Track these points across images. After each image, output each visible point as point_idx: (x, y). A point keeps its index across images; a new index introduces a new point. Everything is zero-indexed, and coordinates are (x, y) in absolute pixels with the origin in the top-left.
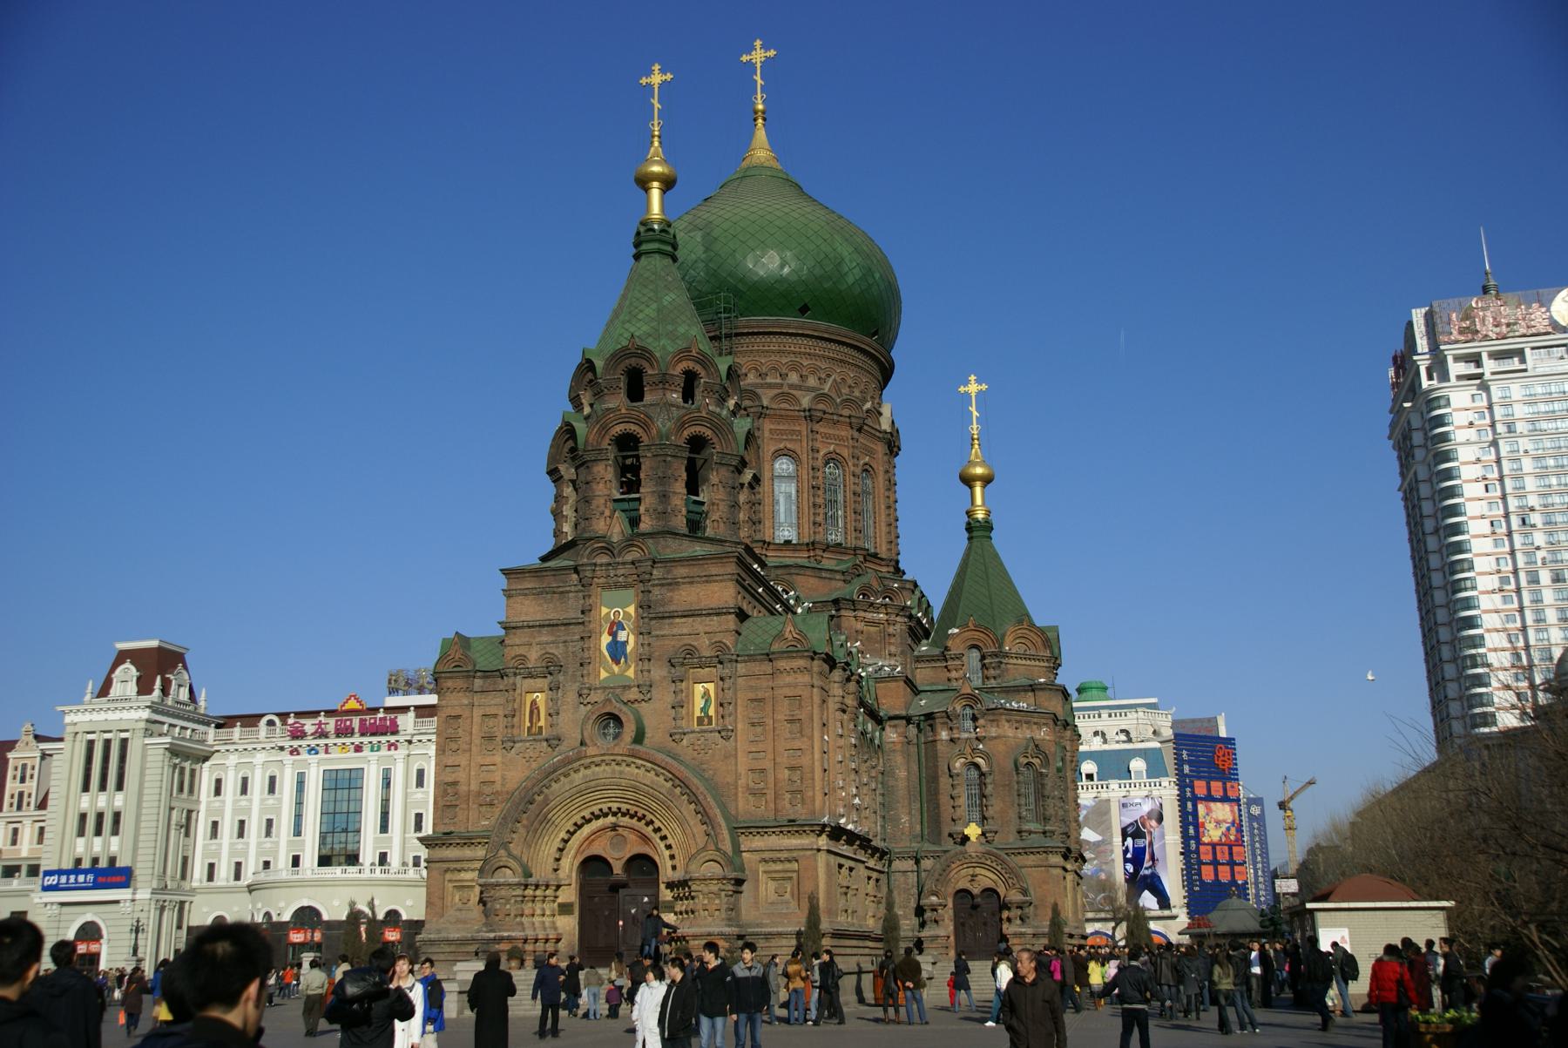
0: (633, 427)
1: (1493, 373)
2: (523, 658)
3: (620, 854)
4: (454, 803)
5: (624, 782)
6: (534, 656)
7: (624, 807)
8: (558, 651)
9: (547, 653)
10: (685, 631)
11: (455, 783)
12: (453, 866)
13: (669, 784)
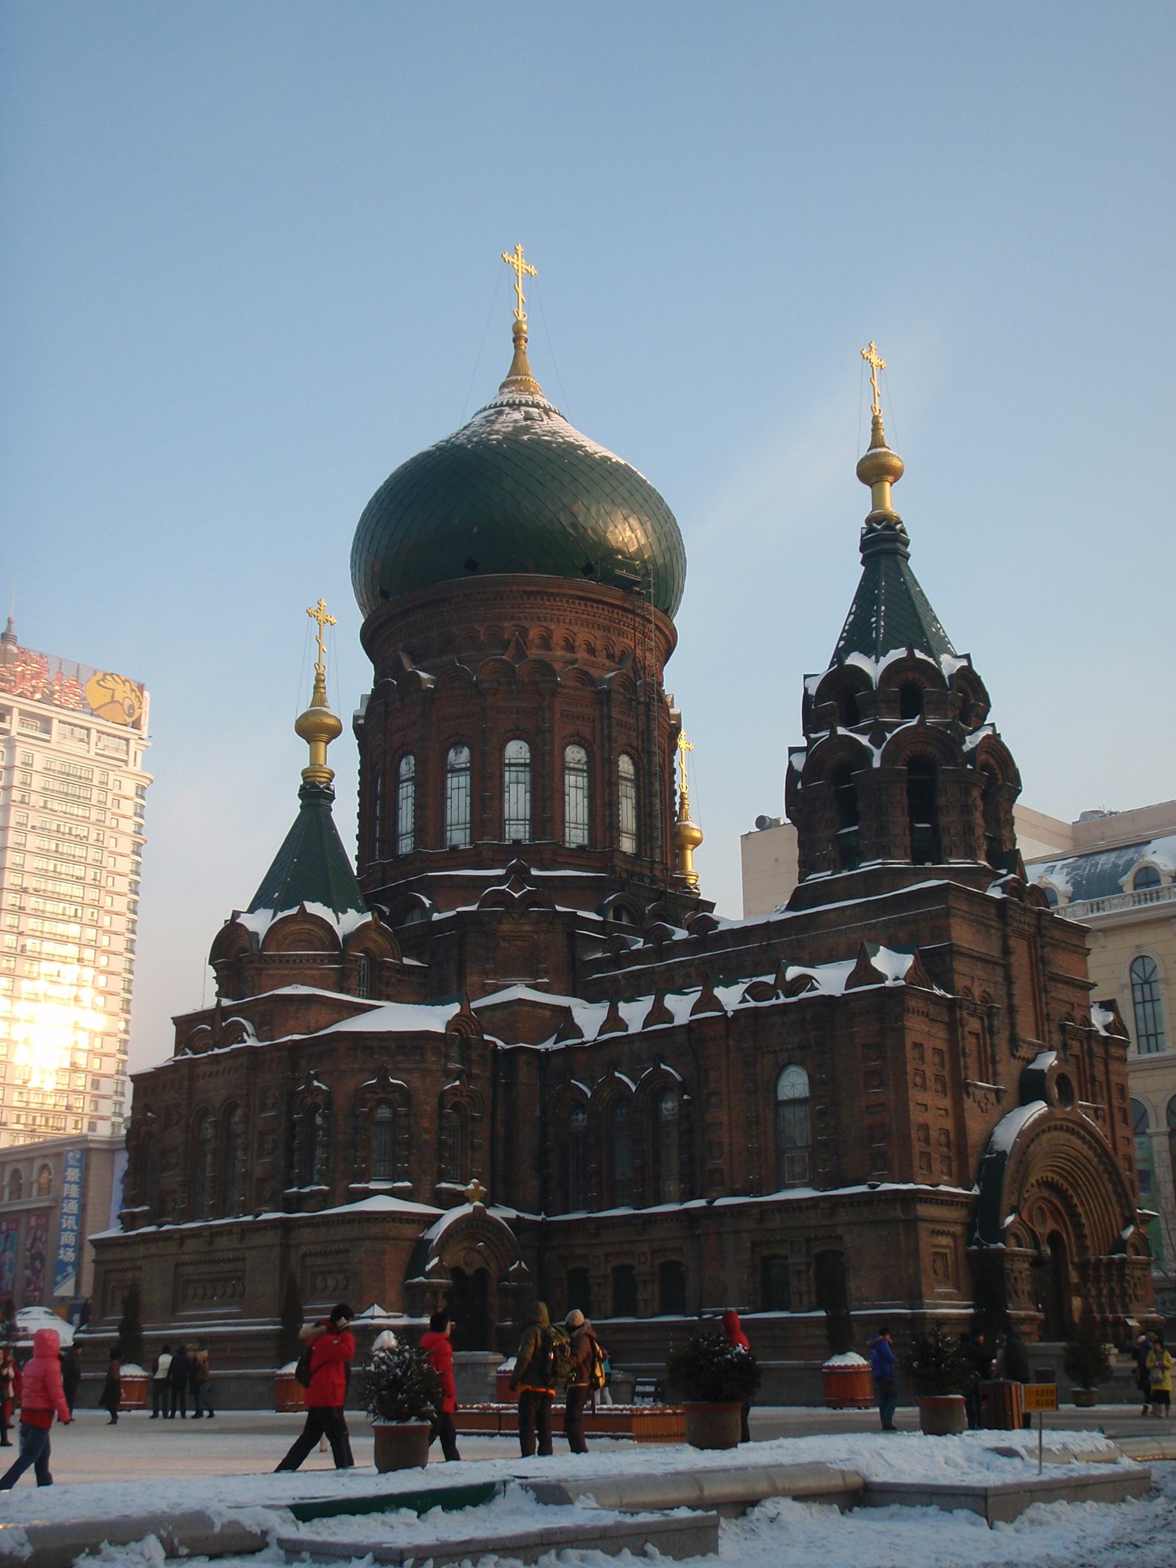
0: (993, 762)
1: (19, 734)
2: (968, 991)
3: (1042, 1231)
4: (927, 1150)
5: (1072, 1152)
6: (977, 991)
7: (1056, 1178)
8: (991, 991)
9: (985, 991)
10: (1064, 998)
11: (925, 1127)
12: (938, 1227)
13: (1096, 1160)
